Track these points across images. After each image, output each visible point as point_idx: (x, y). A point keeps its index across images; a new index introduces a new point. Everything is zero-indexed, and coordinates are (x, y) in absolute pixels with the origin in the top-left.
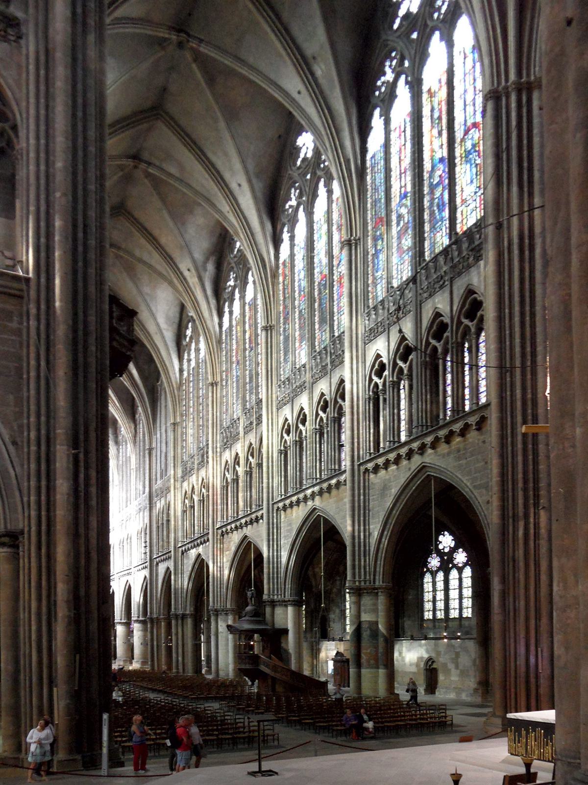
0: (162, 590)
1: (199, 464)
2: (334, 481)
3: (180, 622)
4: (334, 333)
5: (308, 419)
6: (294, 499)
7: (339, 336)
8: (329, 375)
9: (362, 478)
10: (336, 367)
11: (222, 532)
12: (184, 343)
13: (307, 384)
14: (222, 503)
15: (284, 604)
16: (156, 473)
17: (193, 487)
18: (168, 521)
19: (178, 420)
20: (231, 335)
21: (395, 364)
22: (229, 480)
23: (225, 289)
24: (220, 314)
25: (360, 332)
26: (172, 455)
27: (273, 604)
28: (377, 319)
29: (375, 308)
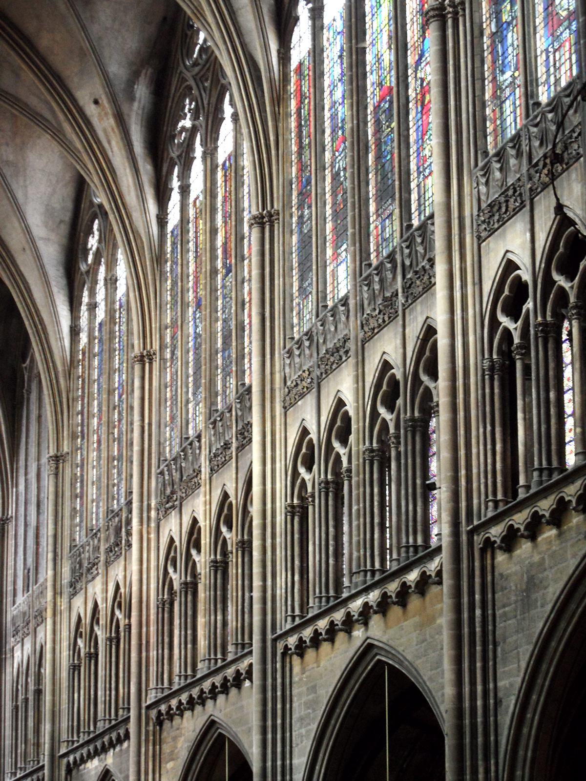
1: (110, 550)
2: (413, 576)
4: (410, 219)
5: (354, 427)
6: (322, 624)
7: (423, 227)
8: (400, 318)
9: (477, 564)
10: (415, 299)
12: (83, 267)
13: (351, 345)
14: (160, 643)
16: (15, 576)
17: (96, 605)
18: (39, 692)
19: (66, 449)
20: (184, 242)
21: (548, 282)
22: (176, 586)
23: (173, 137)
24: (162, 197)
25: (467, 213)
26: (51, 532)
28: (505, 179)
29: (500, 155)
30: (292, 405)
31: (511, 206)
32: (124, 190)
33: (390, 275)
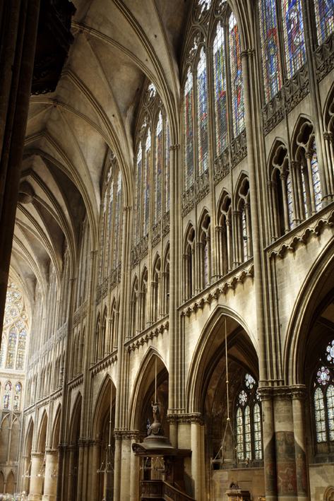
0: (72, 418)
1: (112, 285)
3: (86, 449)
7: (239, 137)
8: (230, 173)
11: (129, 347)
12: (106, 183)
13: (210, 188)
14: (130, 319)
15: (188, 420)
18: (82, 345)
19: (97, 249)
20: (143, 165)
22: (137, 295)
23: (140, 131)
24: (136, 152)
25: (258, 126)
26: (90, 280)
27: (177, 420)
30: (185, 216)
31: (278, 119)
32: (122, 148)
33: (225, 158)
